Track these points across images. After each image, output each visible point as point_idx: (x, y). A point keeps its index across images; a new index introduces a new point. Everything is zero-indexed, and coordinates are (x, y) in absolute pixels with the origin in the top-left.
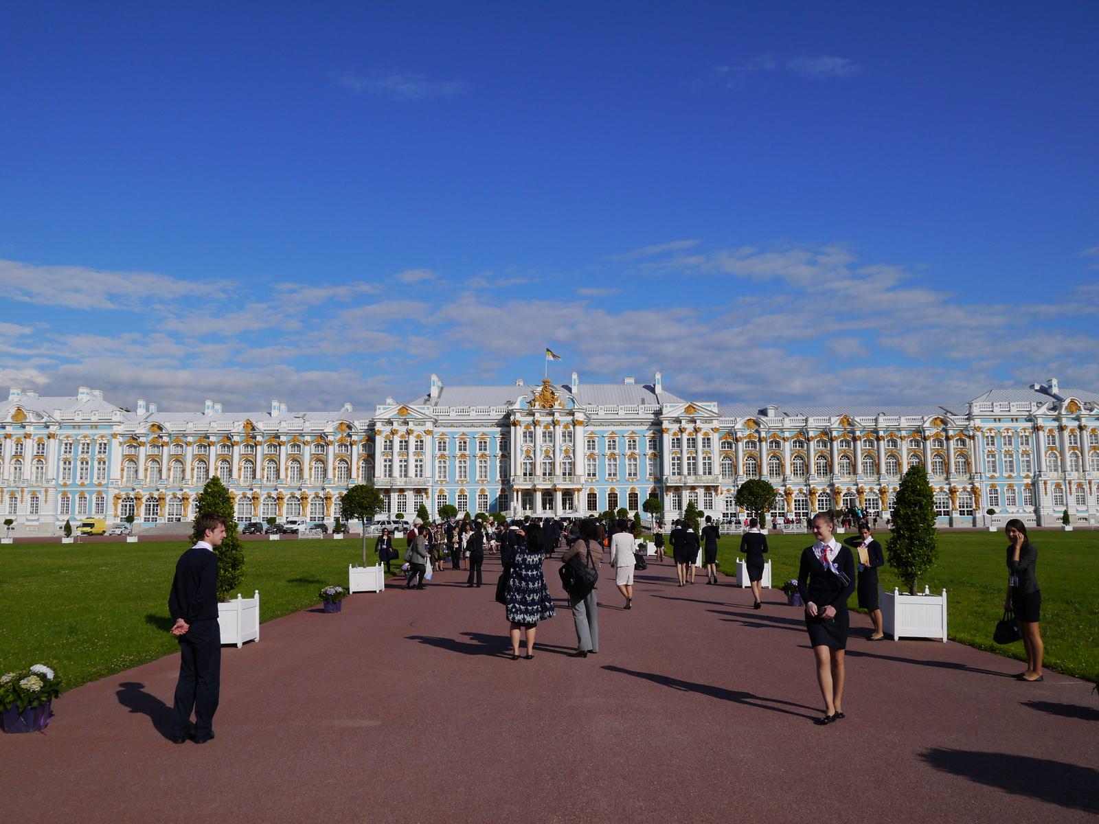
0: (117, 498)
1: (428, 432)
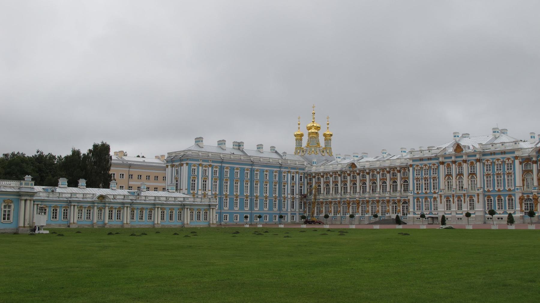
0: (521, 199)
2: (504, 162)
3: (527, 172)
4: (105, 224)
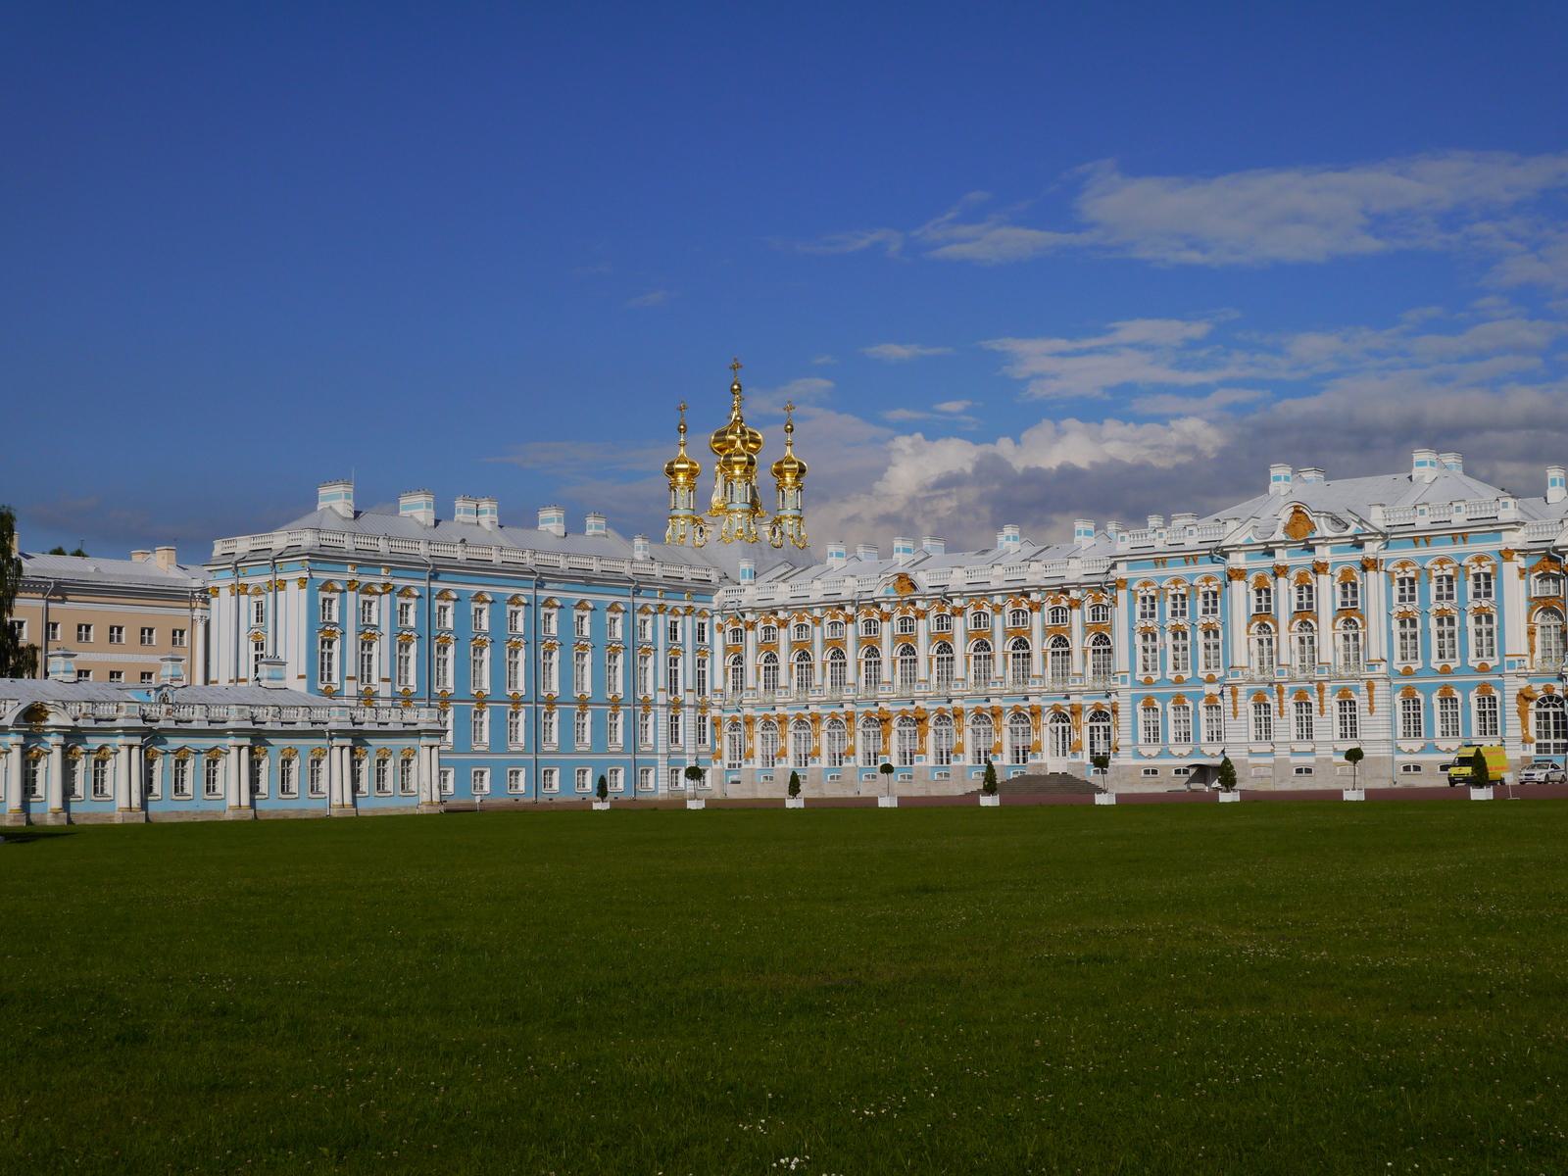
0: (1524, 697)
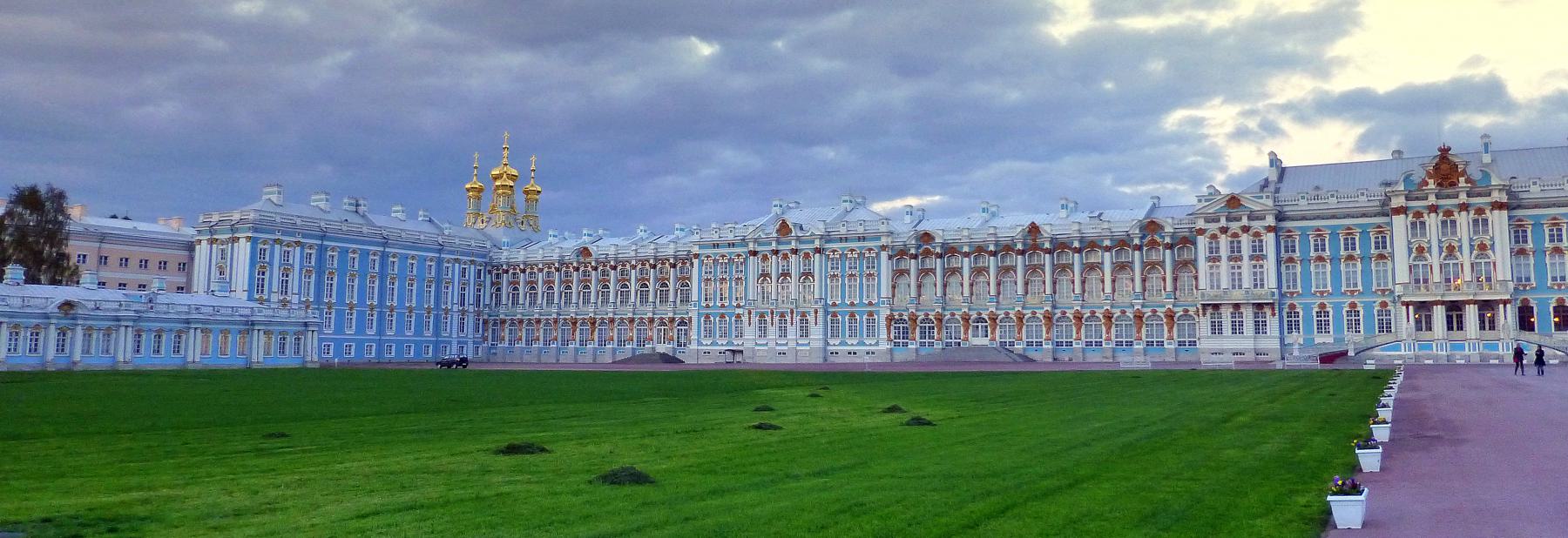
1: (1269, 229)
2: (861, 255)
3: (900, 273)
4: (75, 363)
